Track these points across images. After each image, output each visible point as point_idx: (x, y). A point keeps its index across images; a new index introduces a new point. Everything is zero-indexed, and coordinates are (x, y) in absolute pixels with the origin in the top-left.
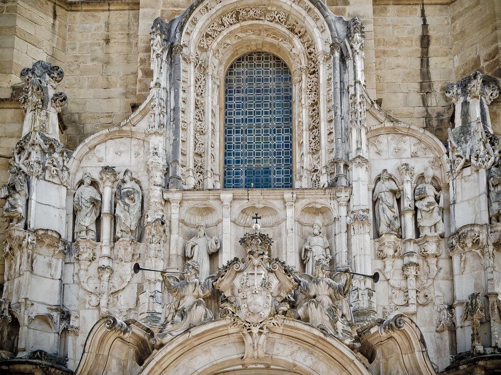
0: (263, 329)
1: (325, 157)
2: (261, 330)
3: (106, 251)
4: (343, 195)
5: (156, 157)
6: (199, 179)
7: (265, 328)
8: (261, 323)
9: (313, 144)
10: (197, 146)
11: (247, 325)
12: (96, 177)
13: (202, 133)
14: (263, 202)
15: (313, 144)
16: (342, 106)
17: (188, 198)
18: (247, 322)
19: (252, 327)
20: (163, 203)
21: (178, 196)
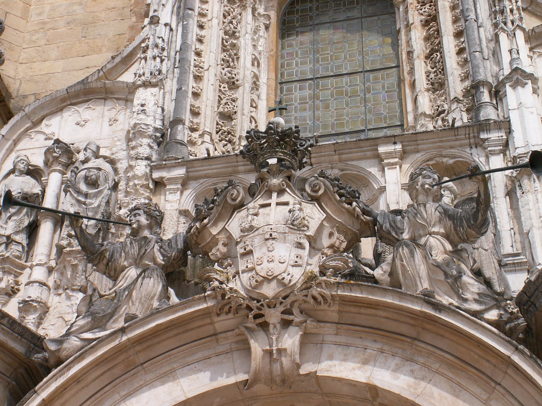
0: (293, 314)
1: (456, 86)
2: (286, 317)
3: (39, 274)
4: (495, 135)
5: (142, 116)
6: (224, 150)
7: (295, 311)
8: (285, 298)
9: (432, 75)
10: (224, 102)
11: (254, 304)
12: (38, 160)
13: (233, 85)
14: (340, 165)
15: (432, 75)
16: (478, 6)
17: (196, 174)
18: (254, 299)
19: (266, 311)
20: (151, 186)
21: (180, 172)
